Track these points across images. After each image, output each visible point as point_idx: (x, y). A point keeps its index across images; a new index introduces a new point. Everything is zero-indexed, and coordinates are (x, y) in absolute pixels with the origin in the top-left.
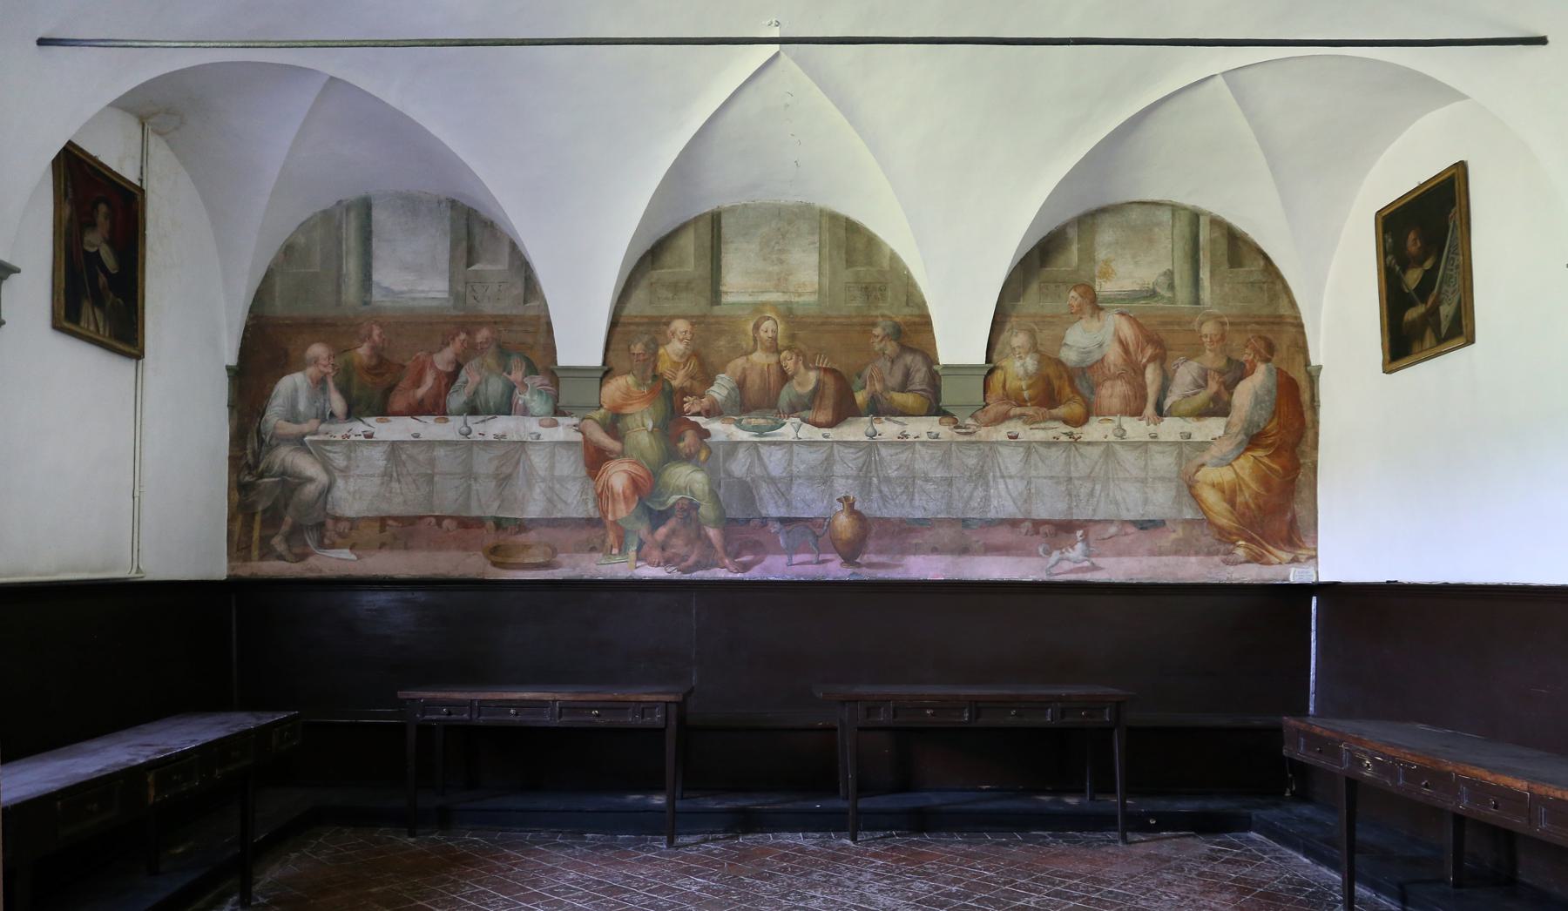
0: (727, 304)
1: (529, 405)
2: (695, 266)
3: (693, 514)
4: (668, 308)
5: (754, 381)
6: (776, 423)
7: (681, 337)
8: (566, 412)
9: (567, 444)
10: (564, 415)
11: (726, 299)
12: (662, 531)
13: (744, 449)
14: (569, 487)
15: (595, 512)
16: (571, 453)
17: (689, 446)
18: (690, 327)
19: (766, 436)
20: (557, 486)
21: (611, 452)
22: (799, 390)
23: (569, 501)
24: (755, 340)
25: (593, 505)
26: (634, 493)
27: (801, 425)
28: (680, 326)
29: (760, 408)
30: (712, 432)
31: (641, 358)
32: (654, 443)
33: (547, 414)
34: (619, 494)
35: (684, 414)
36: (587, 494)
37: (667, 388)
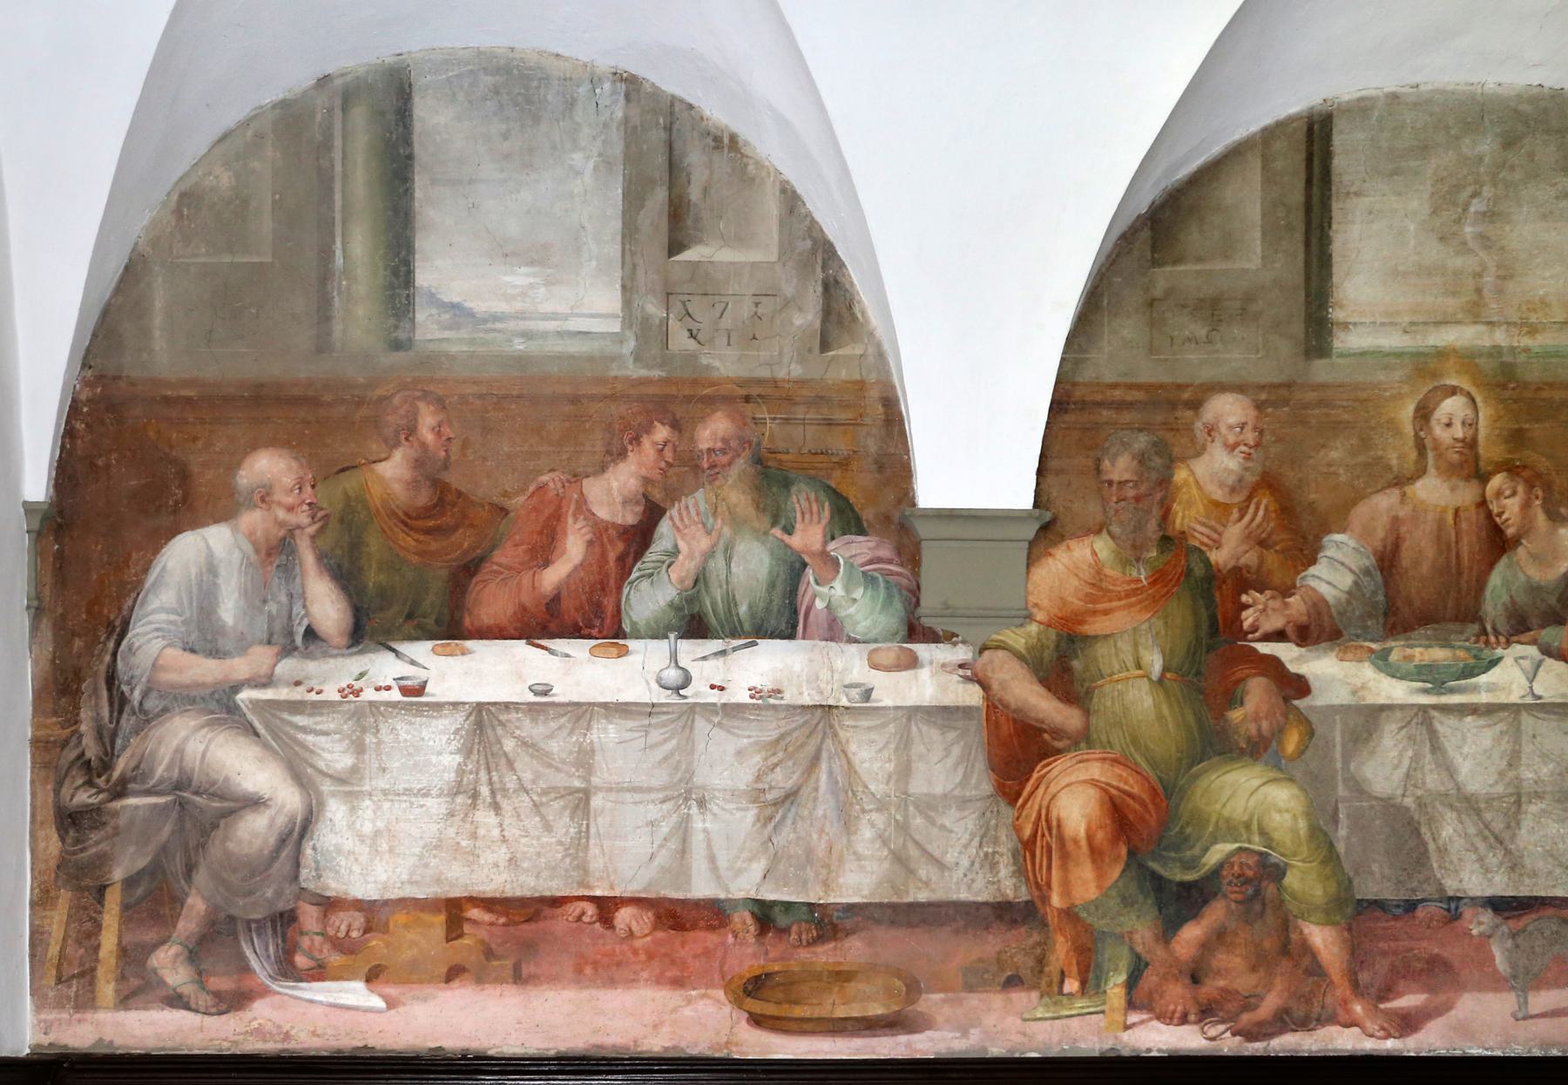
0: (1341, 355)
1: (842, 613)
2: (1263, 258)
3: (1270, 890)
4: (1195, 365)
5: (1421, 551)
6: (1475, 657)
7: (1231, 439)
8: (939, 629)
9: (943, 715)
10: (932, 637)
11: (1349, 341)
12: (1191, 933)
13: (1394, 727)
14: (948, 824)
15: (1016, 888)
16: (952, 735)
17: (1257, 719)
18: (1253, 413)
19: (1452, 691)
20: (918, 821)
21: (1057, 733)
22: (1535, 574)
23: (949, 858)
24: (1421, 447)
25: (1011, 869)
26: (1115, 840)
27: (1539, 665)
28: (1228, 410)
29: (1437, 622)
30: (1314, 684)
31: (1131, 493)
32: (1166, 711)
33: (890, 637)
34: (1076, 842)
35: (1244, 635)
36: (996, 841)
37: (1199, 571)
